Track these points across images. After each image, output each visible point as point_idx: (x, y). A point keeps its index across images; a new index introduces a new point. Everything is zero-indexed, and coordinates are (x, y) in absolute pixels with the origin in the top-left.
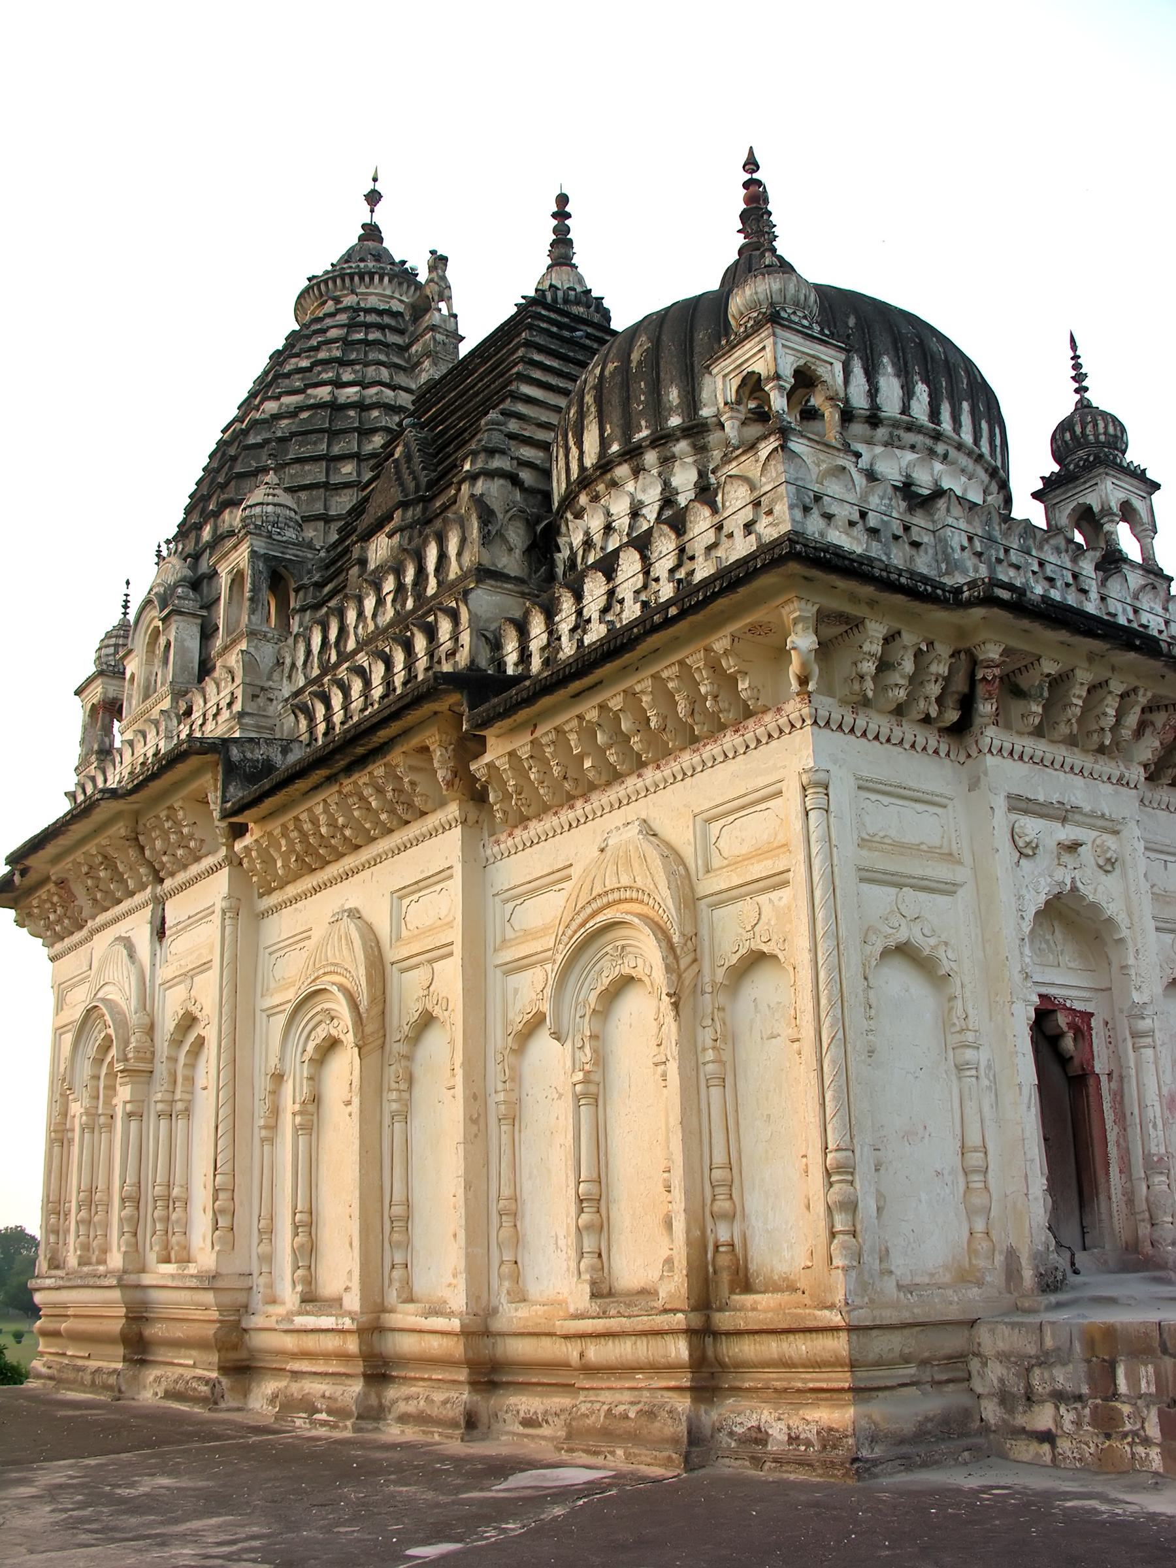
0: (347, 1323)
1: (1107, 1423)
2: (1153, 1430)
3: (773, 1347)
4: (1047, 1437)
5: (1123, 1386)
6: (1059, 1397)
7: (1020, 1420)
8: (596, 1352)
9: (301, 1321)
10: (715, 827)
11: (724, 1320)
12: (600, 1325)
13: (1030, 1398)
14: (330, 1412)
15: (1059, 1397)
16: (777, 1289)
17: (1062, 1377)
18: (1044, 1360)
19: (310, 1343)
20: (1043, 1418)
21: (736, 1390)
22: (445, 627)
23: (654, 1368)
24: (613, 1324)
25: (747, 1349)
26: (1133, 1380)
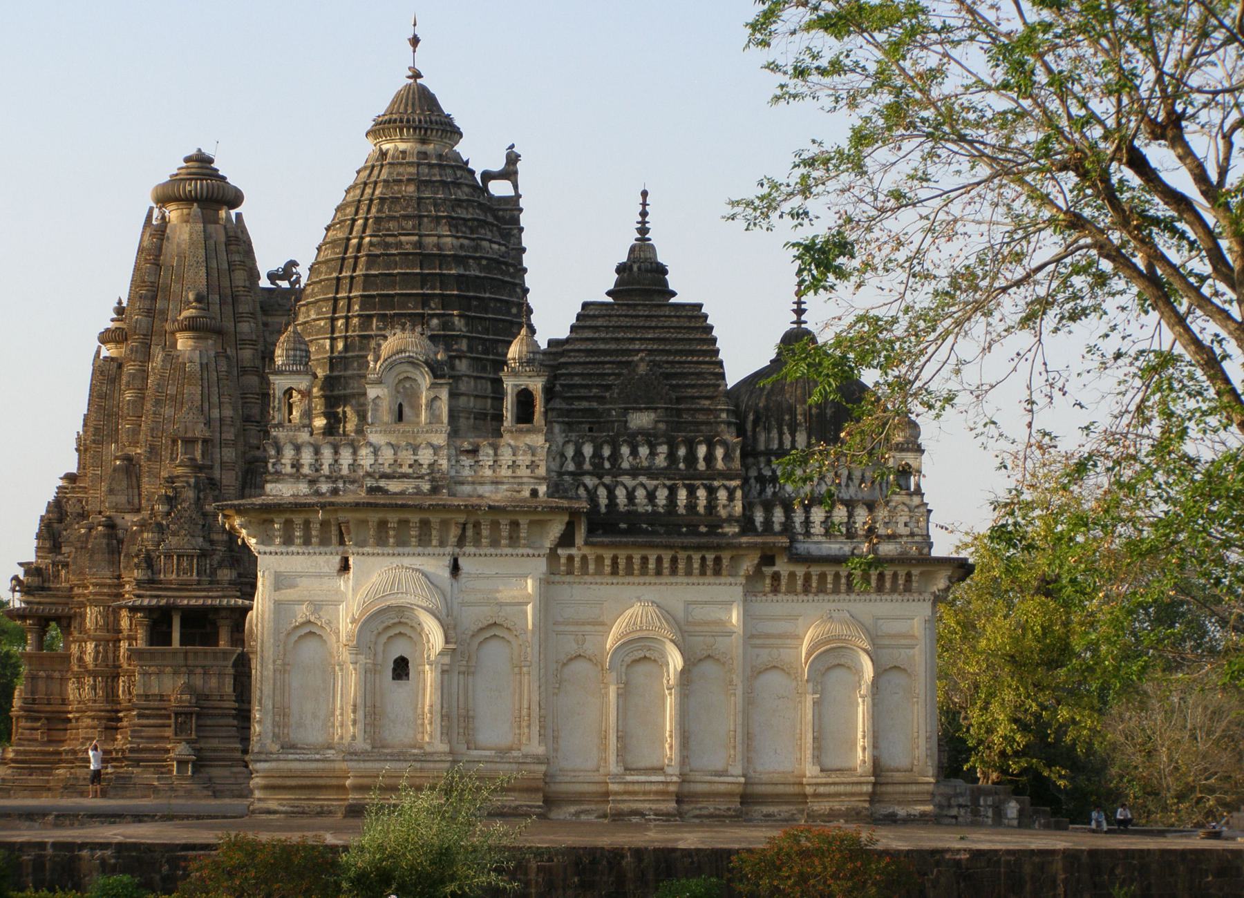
0: (675, 779)
1: (975, 813)
2: (990, 813)
3: (902, 788)
4: (955, 817)
5: (982, 802)
6: (960, 806)
7: (945, 813)
8: (821, 789)
9: (629, 778)
10: (880, 622)
11: (882, 780)
12: (824, 780)
13: (950, 806)
14: (656, 815)
15: (960, 806)
16: (898, 771)
17: (961, 800)
18: (957, 795)
19: (631, 788)
20: (954, 812)
21: (879, 801)
22: (722, 495)
23: (861, 794)
24: (830, 780)
25: (890, 789)
26: (985, 801)
